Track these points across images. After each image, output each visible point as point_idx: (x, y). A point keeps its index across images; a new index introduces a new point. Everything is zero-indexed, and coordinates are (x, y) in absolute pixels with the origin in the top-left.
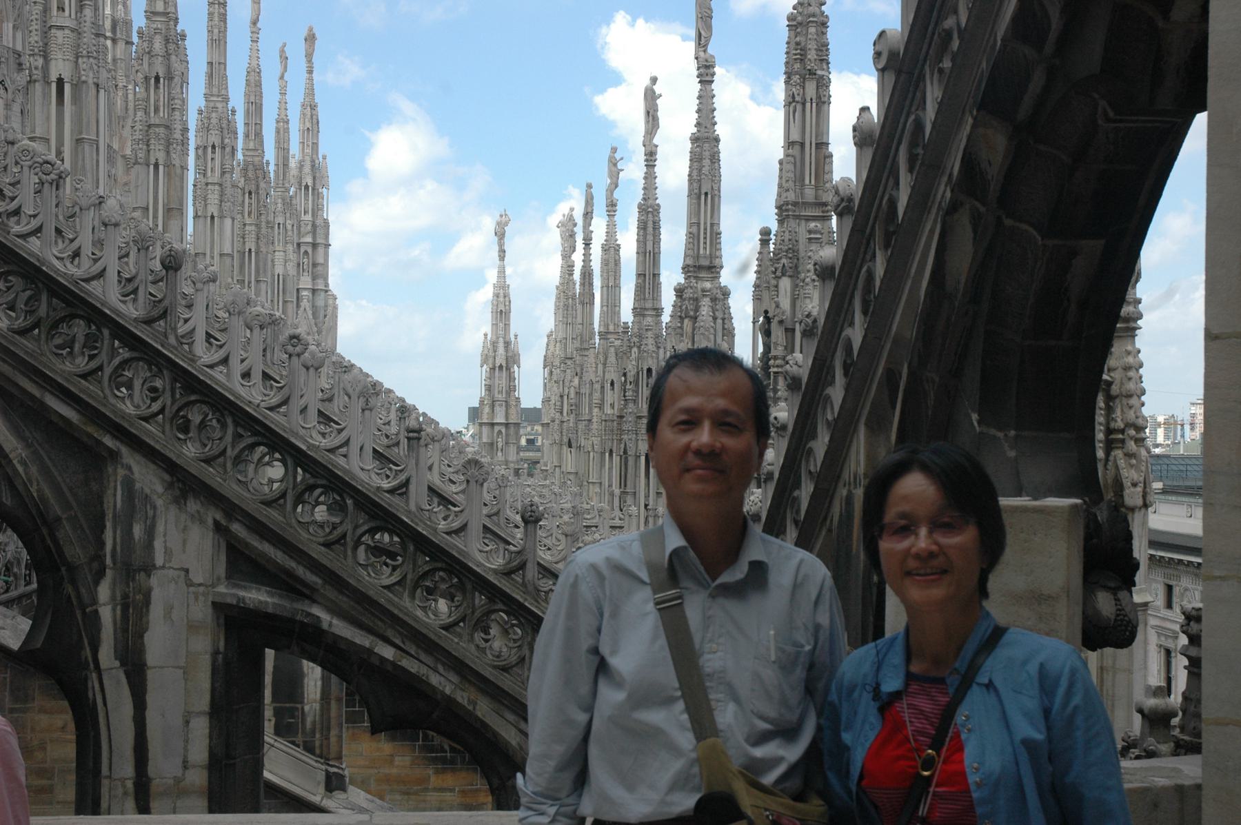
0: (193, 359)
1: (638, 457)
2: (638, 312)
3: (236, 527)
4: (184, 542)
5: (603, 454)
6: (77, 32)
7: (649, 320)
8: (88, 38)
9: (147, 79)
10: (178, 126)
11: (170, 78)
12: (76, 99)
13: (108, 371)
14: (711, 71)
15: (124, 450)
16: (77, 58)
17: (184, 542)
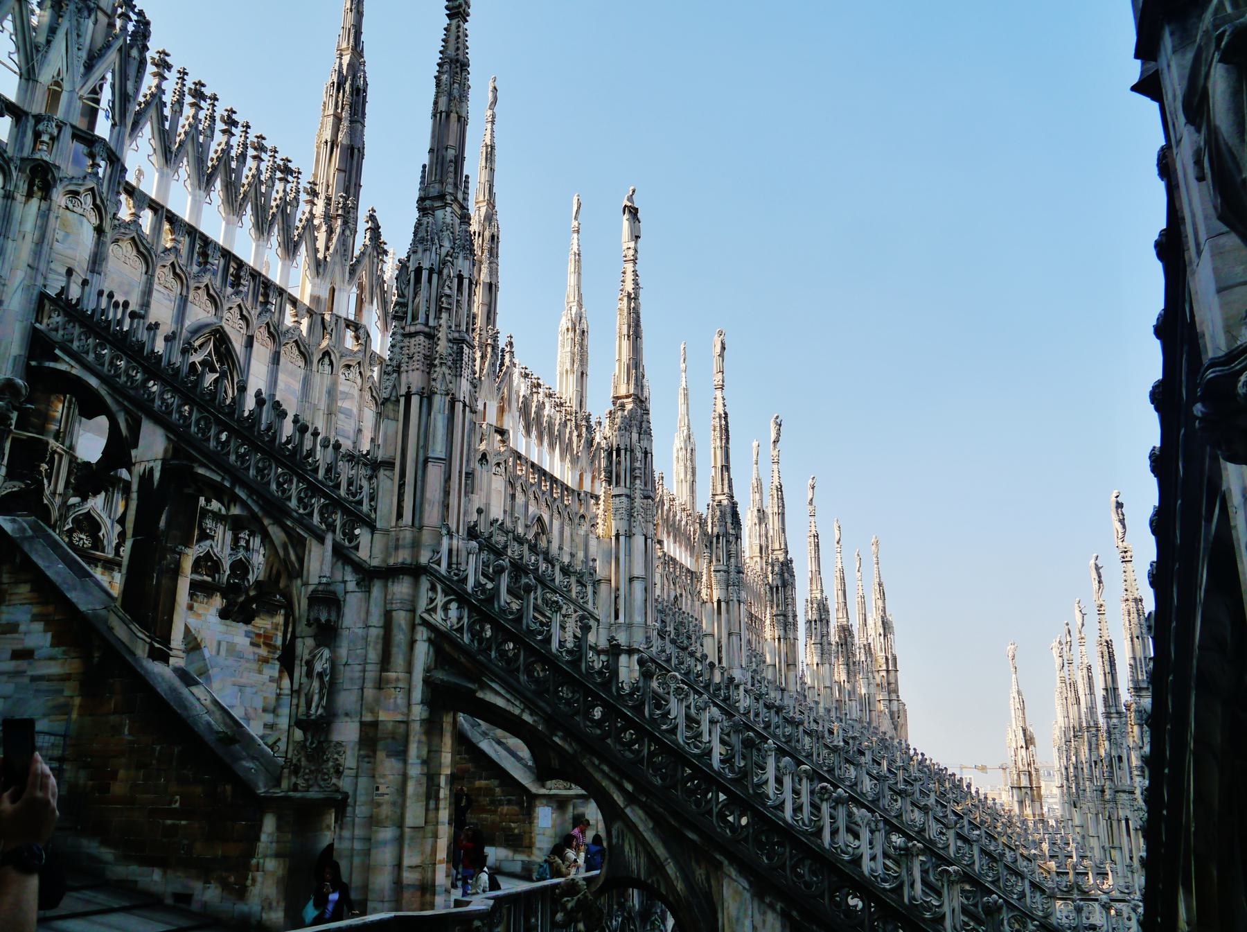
0: (764, 805)
1: (1119, 821)
2: (1108, 715)
3: (794, 913)
4: (764, 922)
5: (1097, 814)
6: (727, 572)
7: (1115, 721)
8: (733, 575)
9: (771, 588)
10: (790, 614)
11: (785, 585)
12: (728, 611)
13: (715, 810)
14: (1129, 554)
15: (726, 863)
16: (728, 586)
17: (764, 922)
